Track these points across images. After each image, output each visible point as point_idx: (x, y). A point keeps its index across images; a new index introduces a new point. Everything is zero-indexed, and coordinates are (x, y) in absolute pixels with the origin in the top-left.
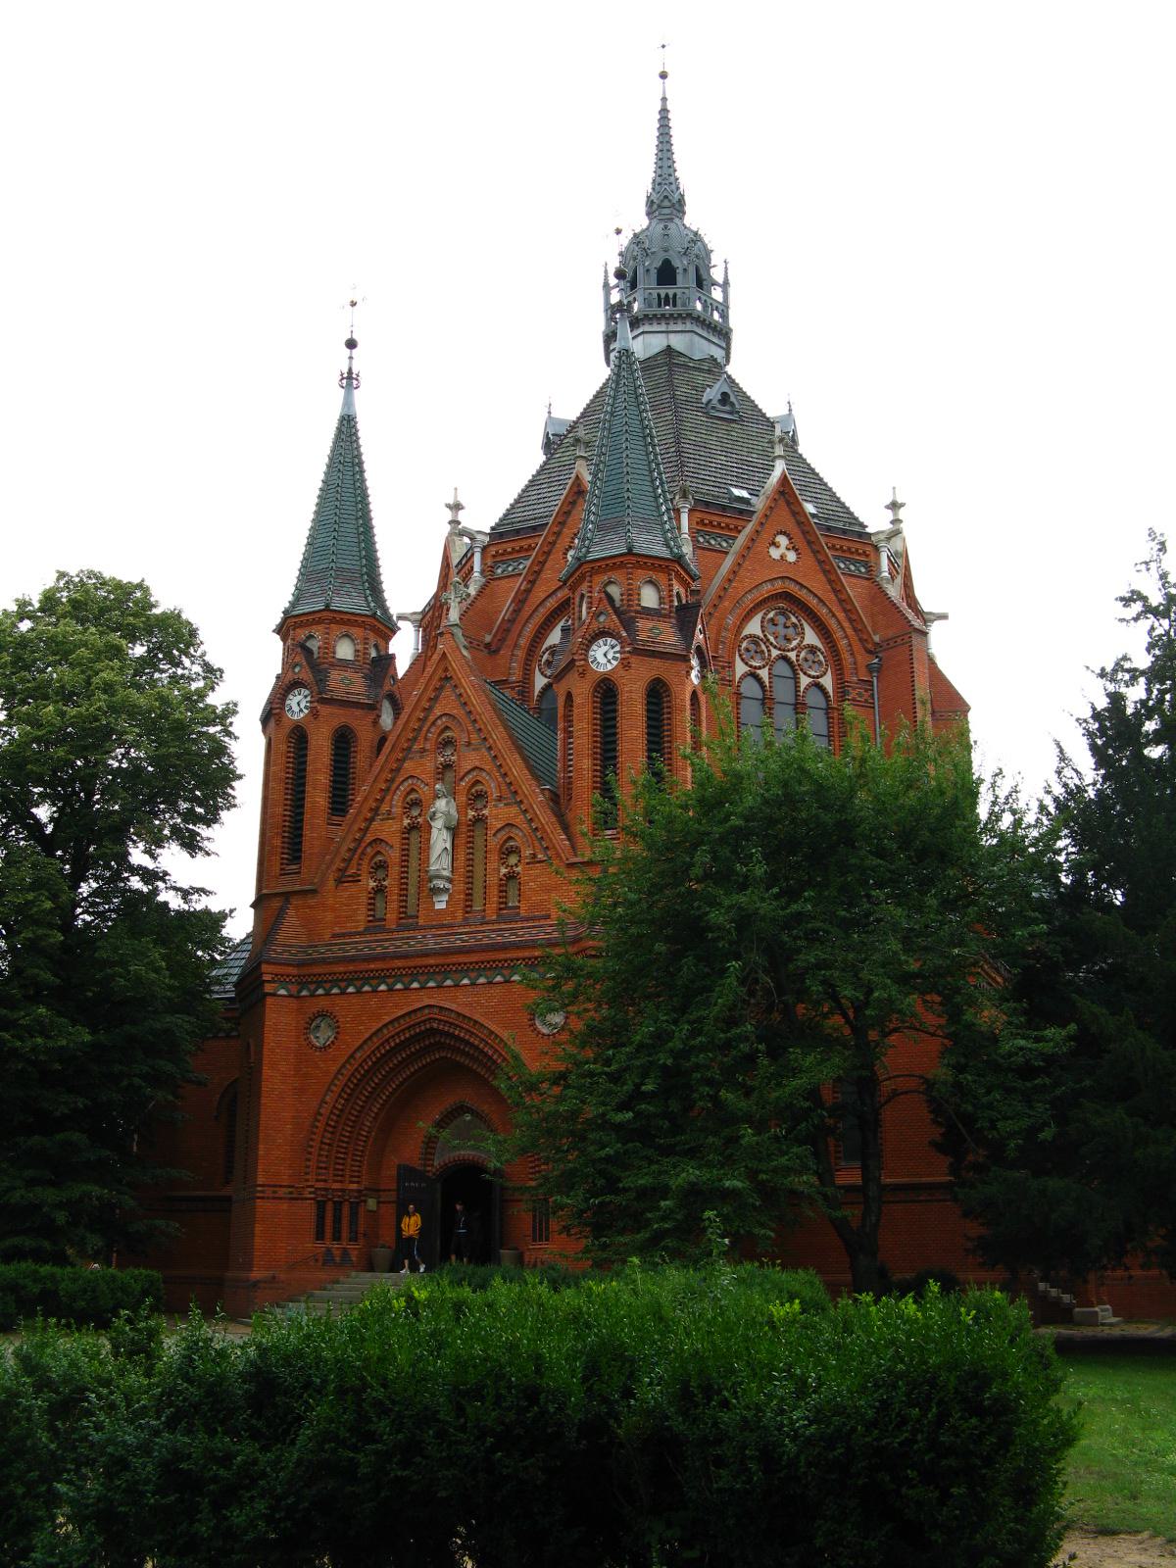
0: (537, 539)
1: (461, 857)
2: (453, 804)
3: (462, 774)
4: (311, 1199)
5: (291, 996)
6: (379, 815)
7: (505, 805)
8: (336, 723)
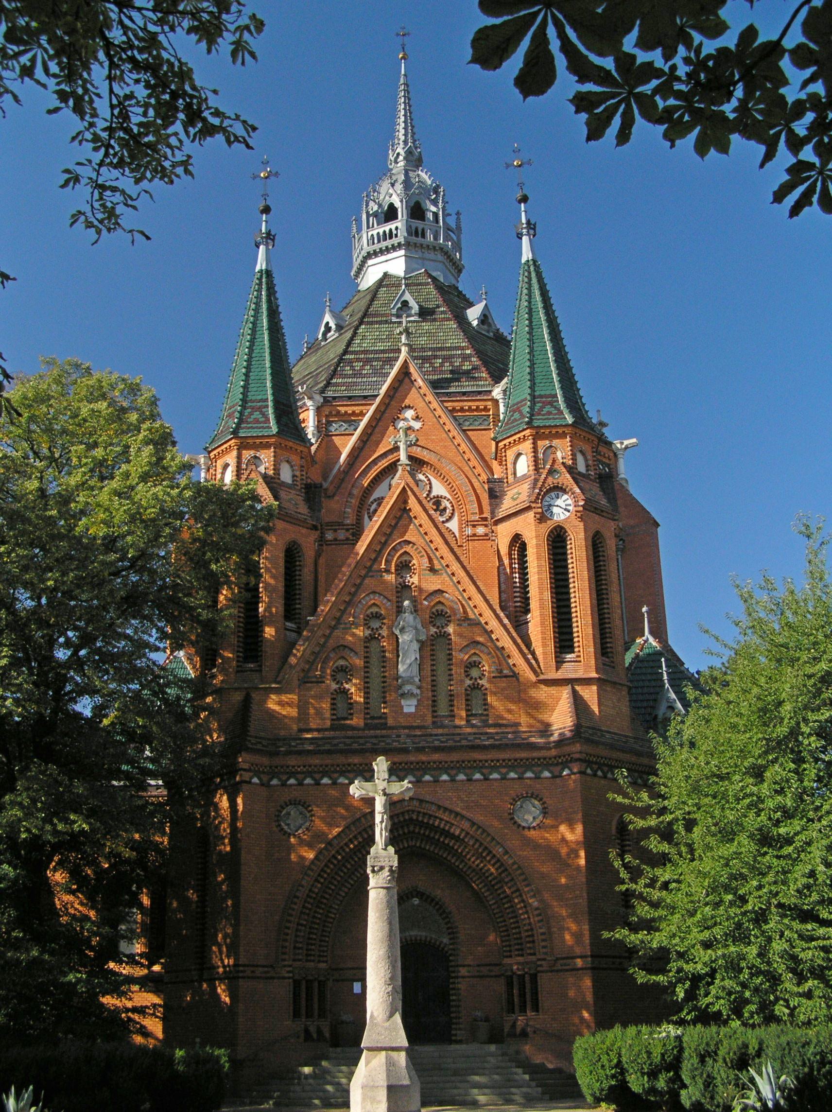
0: (368, 407)
1: (428, 668)
2: (418, 620)
4: (289, 978)
5: (262, 784)
7: (469, 625)
8: (288, 538)
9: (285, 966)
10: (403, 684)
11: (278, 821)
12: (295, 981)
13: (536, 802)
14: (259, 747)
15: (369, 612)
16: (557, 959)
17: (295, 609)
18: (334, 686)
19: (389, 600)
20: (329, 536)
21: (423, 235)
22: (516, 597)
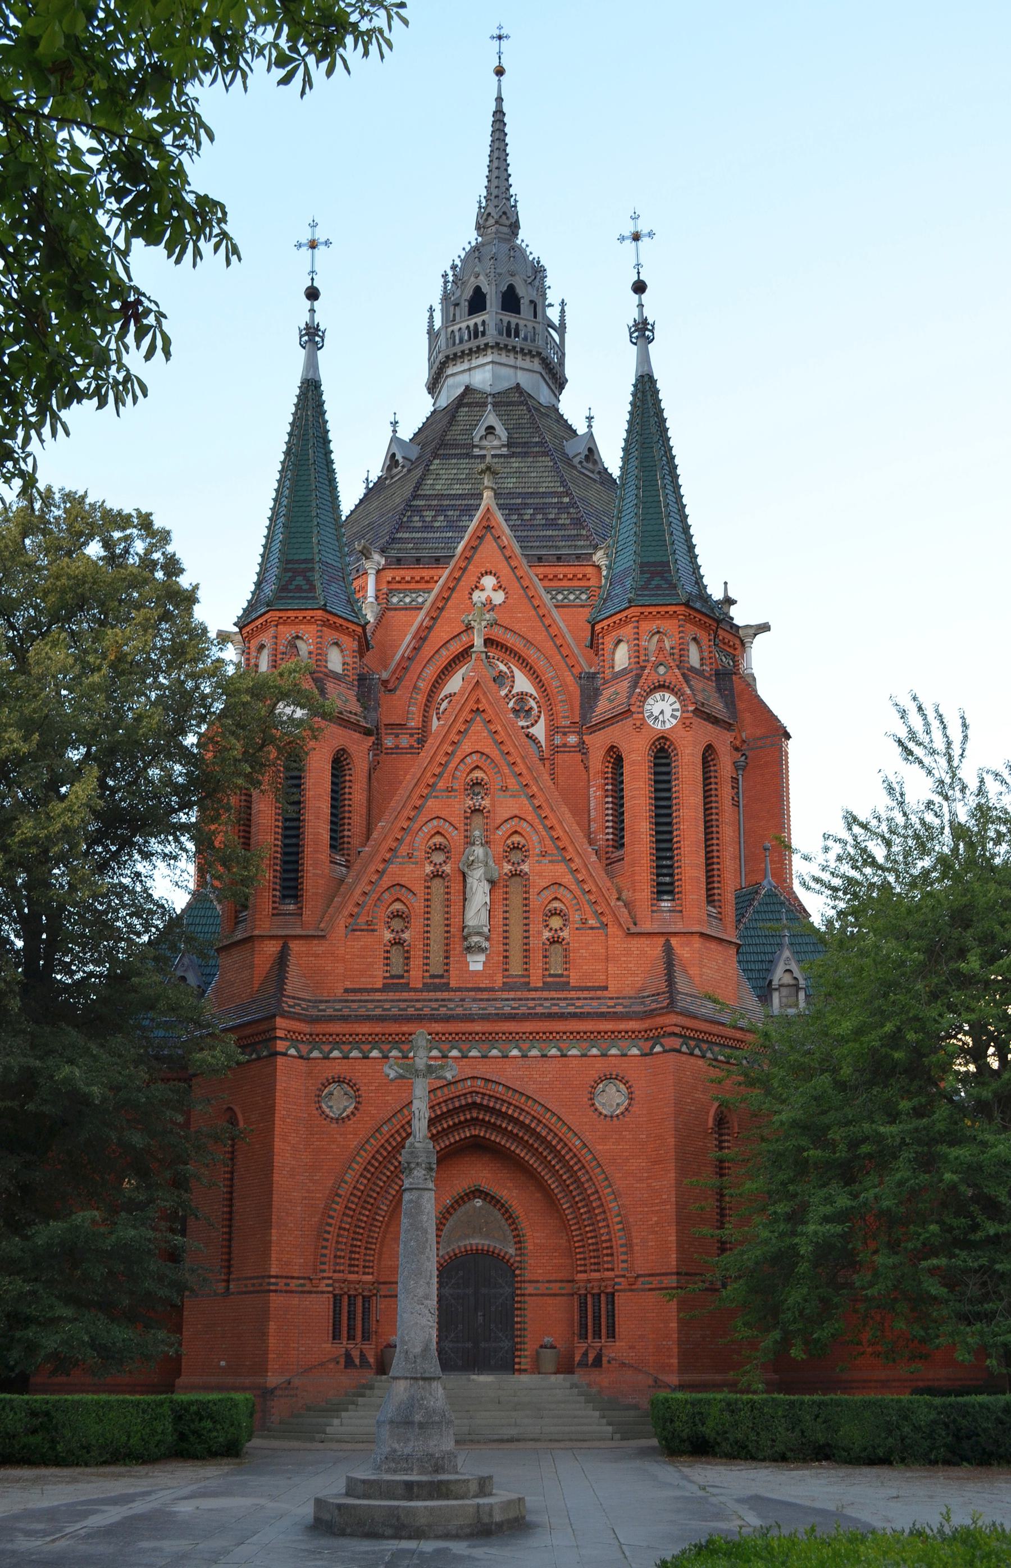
3: (499, 822)
4: (329, 1292)
5: (301, 1057)
6: (398, 857)
7: (550, 862)
9: (324, 1278)
10: (470, 935)
11: (319, 1102)
12: (335, 1296)
13: (622, 1086)
14: (298, 1010)
15: (431, 843)
16: (639, 1276)
17: (343, 837)
20: (389, 742)
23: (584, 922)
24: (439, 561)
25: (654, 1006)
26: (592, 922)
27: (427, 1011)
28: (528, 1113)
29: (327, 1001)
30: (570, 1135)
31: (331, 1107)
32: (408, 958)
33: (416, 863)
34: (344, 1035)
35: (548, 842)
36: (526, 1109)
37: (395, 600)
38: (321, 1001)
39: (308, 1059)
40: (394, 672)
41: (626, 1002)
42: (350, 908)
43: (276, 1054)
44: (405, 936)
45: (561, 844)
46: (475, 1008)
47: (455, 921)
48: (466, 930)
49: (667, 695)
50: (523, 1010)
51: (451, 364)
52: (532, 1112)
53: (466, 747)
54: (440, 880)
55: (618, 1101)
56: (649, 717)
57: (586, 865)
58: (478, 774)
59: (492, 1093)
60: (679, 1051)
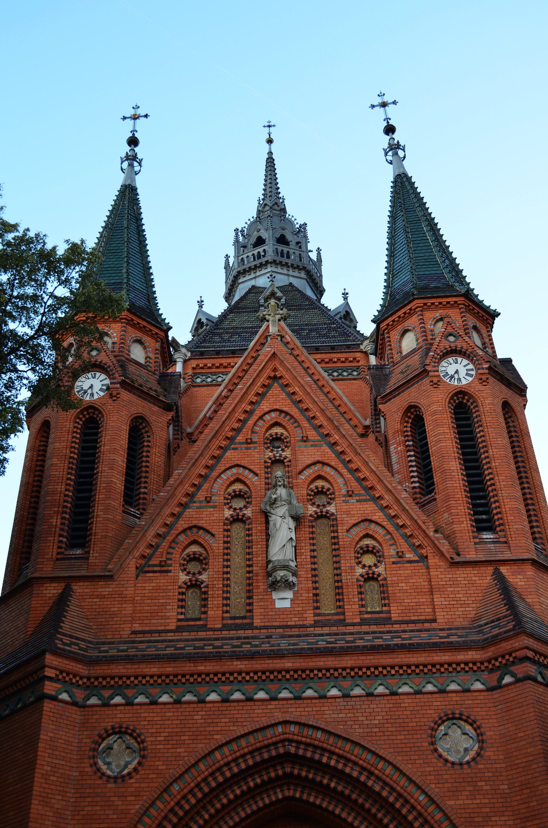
3: (300, 468)
5: (74, 704)
6: (195, 502)
10: (275, 569)
11: (94, 757)
14: (74, 649)
15: (230, 490)
17: (140, 493)
18: (183, 577)
19: (256, 475)
21: (288, 257)
22: (413, 477)
23: (401, 555)
24: (234, 353)
25: (496, 631)
26: (409, 556)
27: (227, 648)
28: (355, 763)
29: (110, 643)
30: (412, 789)
31: (109, 764)
32: (206, 599)
33: (215, 507)
34: (128, 678)
35: (354, 484)
36: (353, 758)
37: (199, 380)
38: (104, 643)
39: (84, 706)
40: (197, 428)
41: (459, 632)
42: (142, 549)
43: (44, 697)
44: (203, 577)
45: (368, 484)
46: (284, 644)
47: (259, 560)
48: (270, 566)
49: (459, 359)
50: (341, 644)
51: (241, 276)
52: (361, 762)
53: (265, 406)
54: (241, 525)
55: (465, 746)
56: (444, 376)
57: (397, 501)
58: (278, 430)
59: (308, 740)
60: (535, 680)
